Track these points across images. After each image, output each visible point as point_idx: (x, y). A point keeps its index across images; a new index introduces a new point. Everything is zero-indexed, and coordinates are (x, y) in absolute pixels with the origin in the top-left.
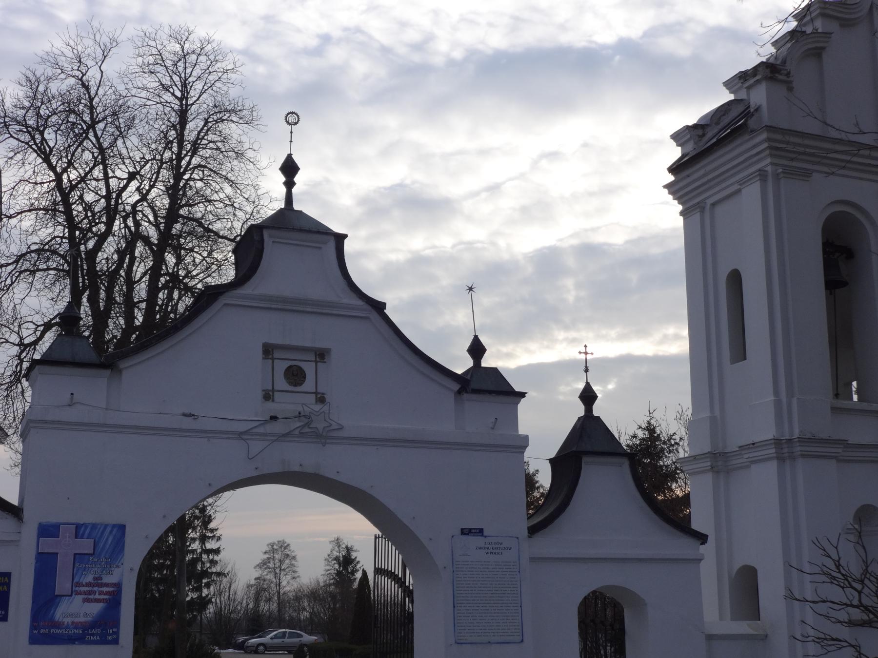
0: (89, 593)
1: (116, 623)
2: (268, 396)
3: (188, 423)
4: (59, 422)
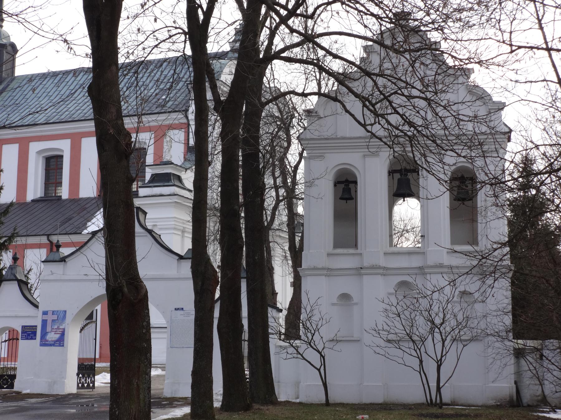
0: (56, 331)
3: (85, 278)
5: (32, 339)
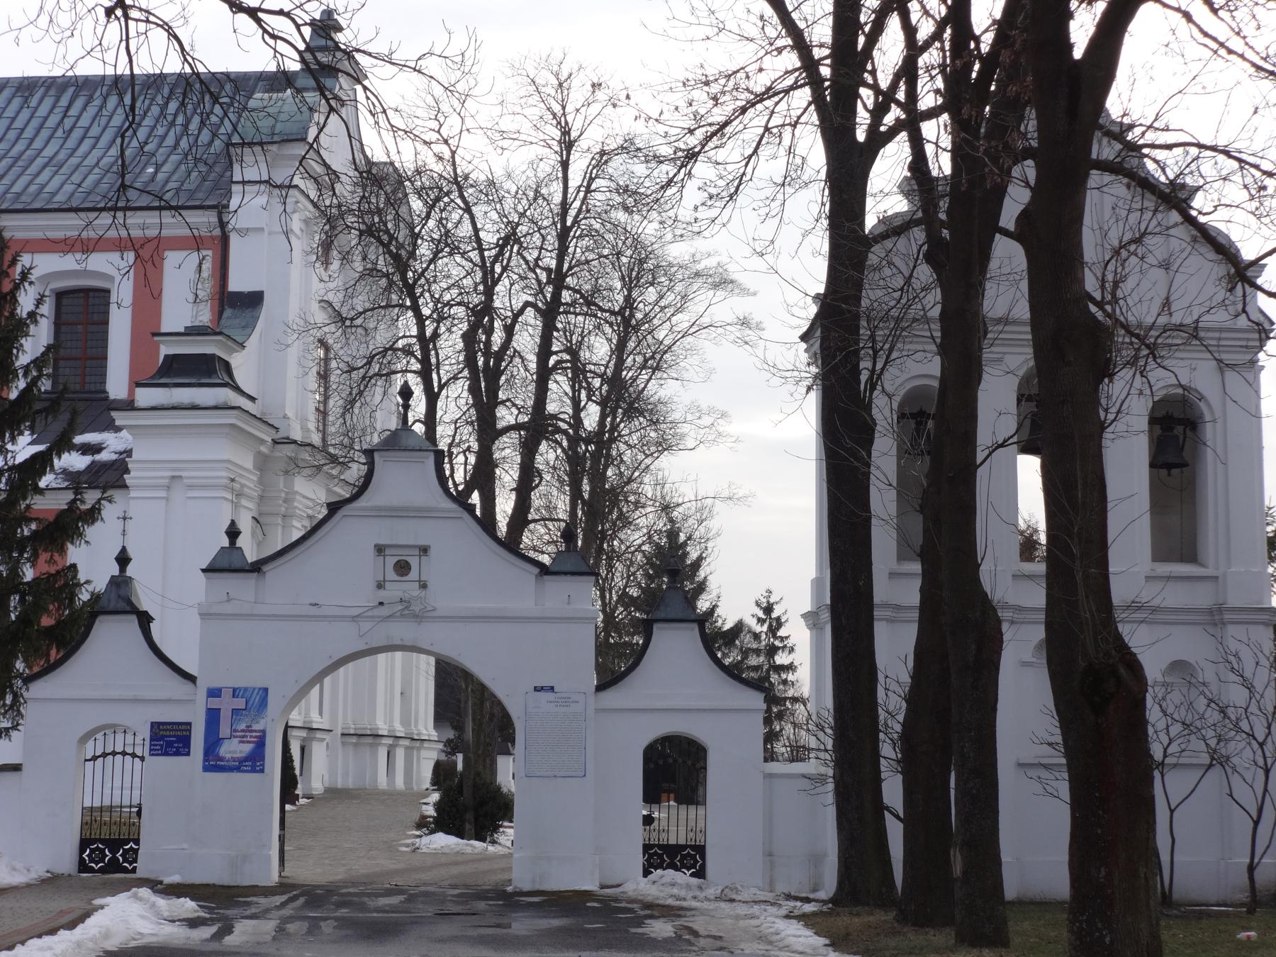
0: (243, 737)
2: (380, 586)
3: (314, 611)
4: (219, 614)
5: (177, 754)
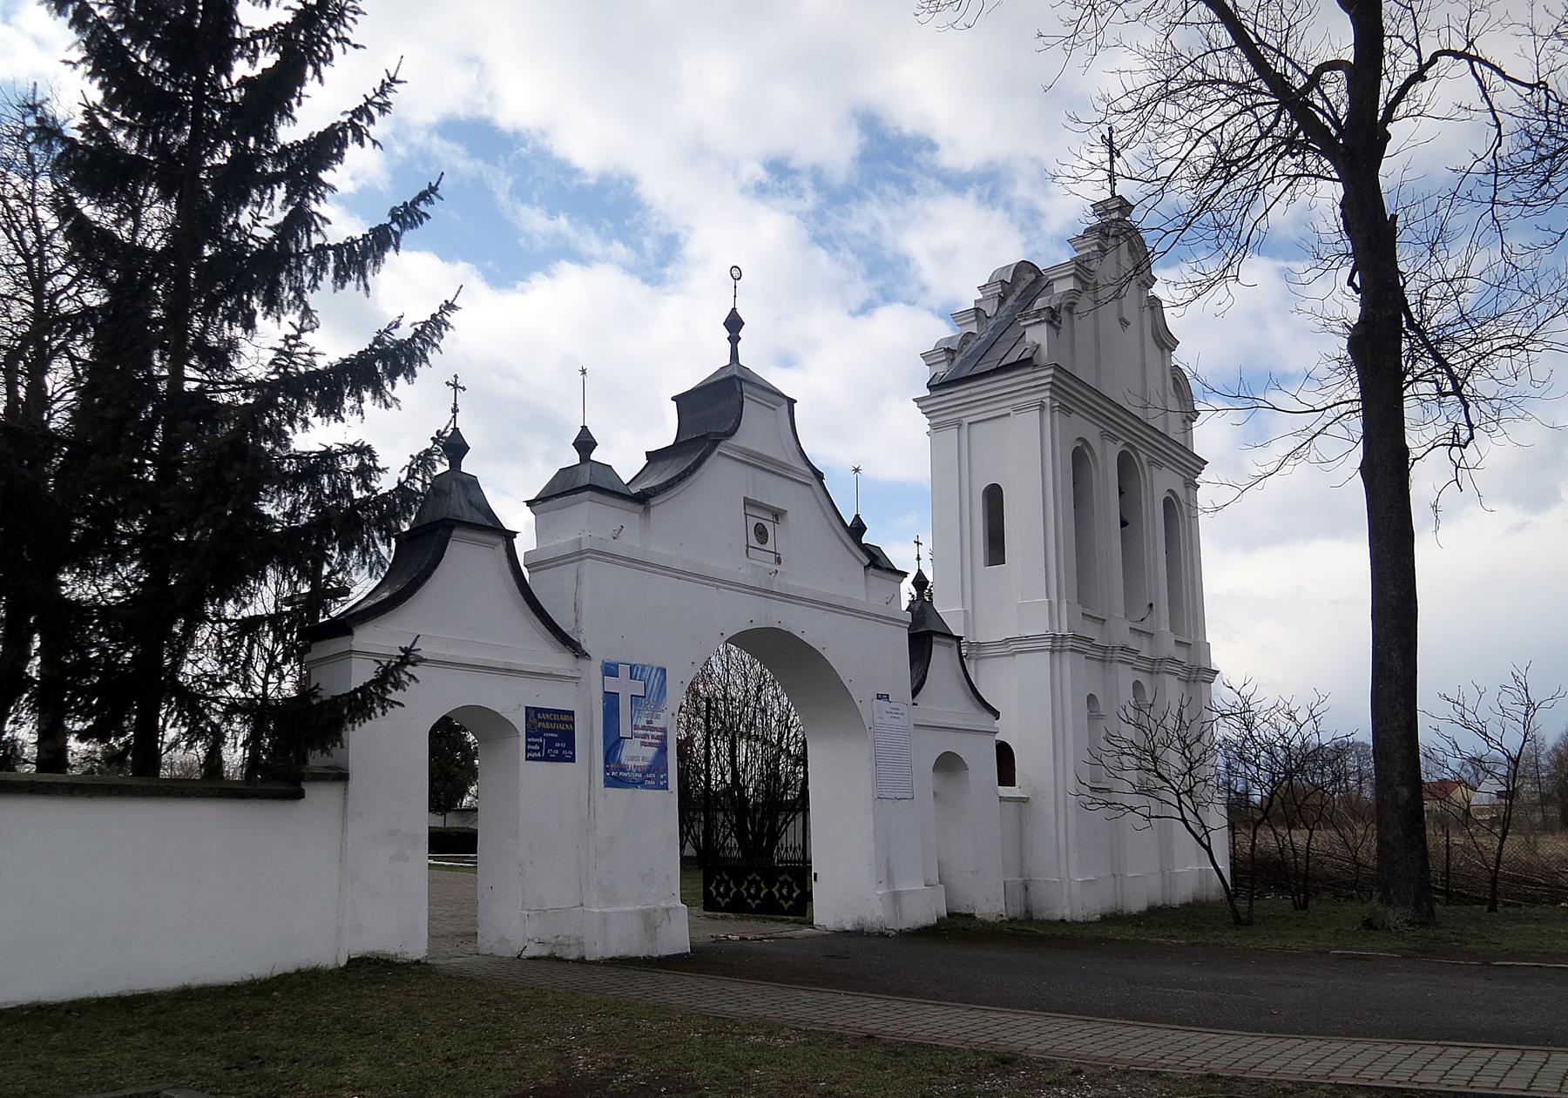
0: (645, 736)
1: (666, 771)
5: (560, 758)
